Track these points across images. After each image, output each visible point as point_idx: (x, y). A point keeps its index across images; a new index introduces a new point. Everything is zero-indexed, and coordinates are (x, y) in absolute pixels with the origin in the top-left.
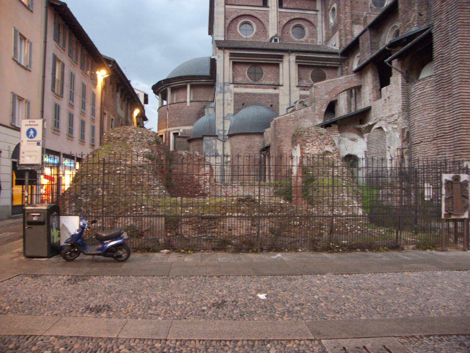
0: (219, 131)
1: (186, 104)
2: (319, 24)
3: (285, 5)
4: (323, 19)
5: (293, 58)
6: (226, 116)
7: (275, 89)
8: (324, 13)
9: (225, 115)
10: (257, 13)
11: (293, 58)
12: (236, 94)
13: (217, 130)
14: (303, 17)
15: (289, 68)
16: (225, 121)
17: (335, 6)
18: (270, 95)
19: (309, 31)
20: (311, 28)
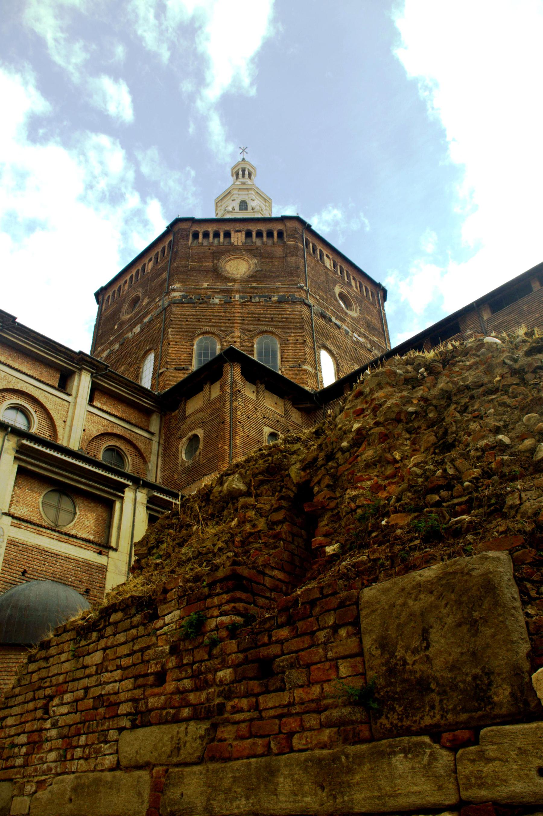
2: (153, 458)
3: (97, 403)
4: (161, 451)
5: (142, 496)
7: (100, 553)
8: (162, 442)
10: (47, 398)
11: (142, 496)
12: (12, 543)
14: (128, 436)
15: (134, 516)
17: (200, 432)
18: (89, 566)
19: (133, 465)
20: (138, 460)
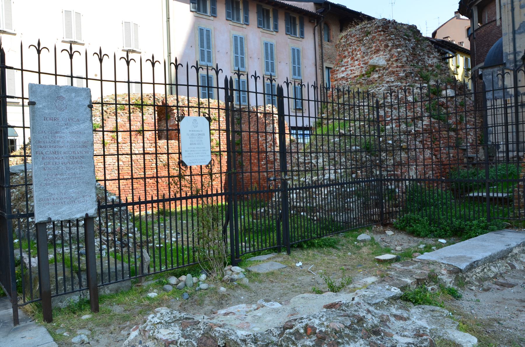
0: (507, 54)
1: (496, 24)
6: (519, 28)
9: (517, 27)
13: (504, 55)
16: (517, 36)
